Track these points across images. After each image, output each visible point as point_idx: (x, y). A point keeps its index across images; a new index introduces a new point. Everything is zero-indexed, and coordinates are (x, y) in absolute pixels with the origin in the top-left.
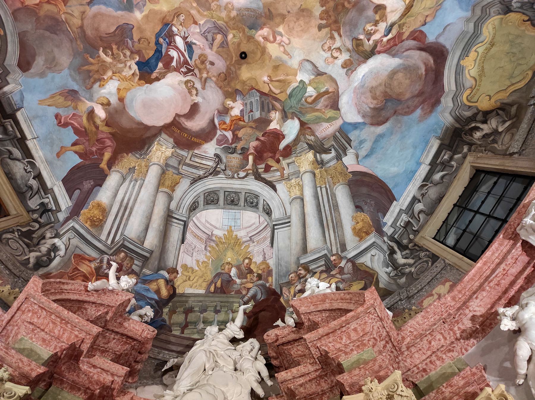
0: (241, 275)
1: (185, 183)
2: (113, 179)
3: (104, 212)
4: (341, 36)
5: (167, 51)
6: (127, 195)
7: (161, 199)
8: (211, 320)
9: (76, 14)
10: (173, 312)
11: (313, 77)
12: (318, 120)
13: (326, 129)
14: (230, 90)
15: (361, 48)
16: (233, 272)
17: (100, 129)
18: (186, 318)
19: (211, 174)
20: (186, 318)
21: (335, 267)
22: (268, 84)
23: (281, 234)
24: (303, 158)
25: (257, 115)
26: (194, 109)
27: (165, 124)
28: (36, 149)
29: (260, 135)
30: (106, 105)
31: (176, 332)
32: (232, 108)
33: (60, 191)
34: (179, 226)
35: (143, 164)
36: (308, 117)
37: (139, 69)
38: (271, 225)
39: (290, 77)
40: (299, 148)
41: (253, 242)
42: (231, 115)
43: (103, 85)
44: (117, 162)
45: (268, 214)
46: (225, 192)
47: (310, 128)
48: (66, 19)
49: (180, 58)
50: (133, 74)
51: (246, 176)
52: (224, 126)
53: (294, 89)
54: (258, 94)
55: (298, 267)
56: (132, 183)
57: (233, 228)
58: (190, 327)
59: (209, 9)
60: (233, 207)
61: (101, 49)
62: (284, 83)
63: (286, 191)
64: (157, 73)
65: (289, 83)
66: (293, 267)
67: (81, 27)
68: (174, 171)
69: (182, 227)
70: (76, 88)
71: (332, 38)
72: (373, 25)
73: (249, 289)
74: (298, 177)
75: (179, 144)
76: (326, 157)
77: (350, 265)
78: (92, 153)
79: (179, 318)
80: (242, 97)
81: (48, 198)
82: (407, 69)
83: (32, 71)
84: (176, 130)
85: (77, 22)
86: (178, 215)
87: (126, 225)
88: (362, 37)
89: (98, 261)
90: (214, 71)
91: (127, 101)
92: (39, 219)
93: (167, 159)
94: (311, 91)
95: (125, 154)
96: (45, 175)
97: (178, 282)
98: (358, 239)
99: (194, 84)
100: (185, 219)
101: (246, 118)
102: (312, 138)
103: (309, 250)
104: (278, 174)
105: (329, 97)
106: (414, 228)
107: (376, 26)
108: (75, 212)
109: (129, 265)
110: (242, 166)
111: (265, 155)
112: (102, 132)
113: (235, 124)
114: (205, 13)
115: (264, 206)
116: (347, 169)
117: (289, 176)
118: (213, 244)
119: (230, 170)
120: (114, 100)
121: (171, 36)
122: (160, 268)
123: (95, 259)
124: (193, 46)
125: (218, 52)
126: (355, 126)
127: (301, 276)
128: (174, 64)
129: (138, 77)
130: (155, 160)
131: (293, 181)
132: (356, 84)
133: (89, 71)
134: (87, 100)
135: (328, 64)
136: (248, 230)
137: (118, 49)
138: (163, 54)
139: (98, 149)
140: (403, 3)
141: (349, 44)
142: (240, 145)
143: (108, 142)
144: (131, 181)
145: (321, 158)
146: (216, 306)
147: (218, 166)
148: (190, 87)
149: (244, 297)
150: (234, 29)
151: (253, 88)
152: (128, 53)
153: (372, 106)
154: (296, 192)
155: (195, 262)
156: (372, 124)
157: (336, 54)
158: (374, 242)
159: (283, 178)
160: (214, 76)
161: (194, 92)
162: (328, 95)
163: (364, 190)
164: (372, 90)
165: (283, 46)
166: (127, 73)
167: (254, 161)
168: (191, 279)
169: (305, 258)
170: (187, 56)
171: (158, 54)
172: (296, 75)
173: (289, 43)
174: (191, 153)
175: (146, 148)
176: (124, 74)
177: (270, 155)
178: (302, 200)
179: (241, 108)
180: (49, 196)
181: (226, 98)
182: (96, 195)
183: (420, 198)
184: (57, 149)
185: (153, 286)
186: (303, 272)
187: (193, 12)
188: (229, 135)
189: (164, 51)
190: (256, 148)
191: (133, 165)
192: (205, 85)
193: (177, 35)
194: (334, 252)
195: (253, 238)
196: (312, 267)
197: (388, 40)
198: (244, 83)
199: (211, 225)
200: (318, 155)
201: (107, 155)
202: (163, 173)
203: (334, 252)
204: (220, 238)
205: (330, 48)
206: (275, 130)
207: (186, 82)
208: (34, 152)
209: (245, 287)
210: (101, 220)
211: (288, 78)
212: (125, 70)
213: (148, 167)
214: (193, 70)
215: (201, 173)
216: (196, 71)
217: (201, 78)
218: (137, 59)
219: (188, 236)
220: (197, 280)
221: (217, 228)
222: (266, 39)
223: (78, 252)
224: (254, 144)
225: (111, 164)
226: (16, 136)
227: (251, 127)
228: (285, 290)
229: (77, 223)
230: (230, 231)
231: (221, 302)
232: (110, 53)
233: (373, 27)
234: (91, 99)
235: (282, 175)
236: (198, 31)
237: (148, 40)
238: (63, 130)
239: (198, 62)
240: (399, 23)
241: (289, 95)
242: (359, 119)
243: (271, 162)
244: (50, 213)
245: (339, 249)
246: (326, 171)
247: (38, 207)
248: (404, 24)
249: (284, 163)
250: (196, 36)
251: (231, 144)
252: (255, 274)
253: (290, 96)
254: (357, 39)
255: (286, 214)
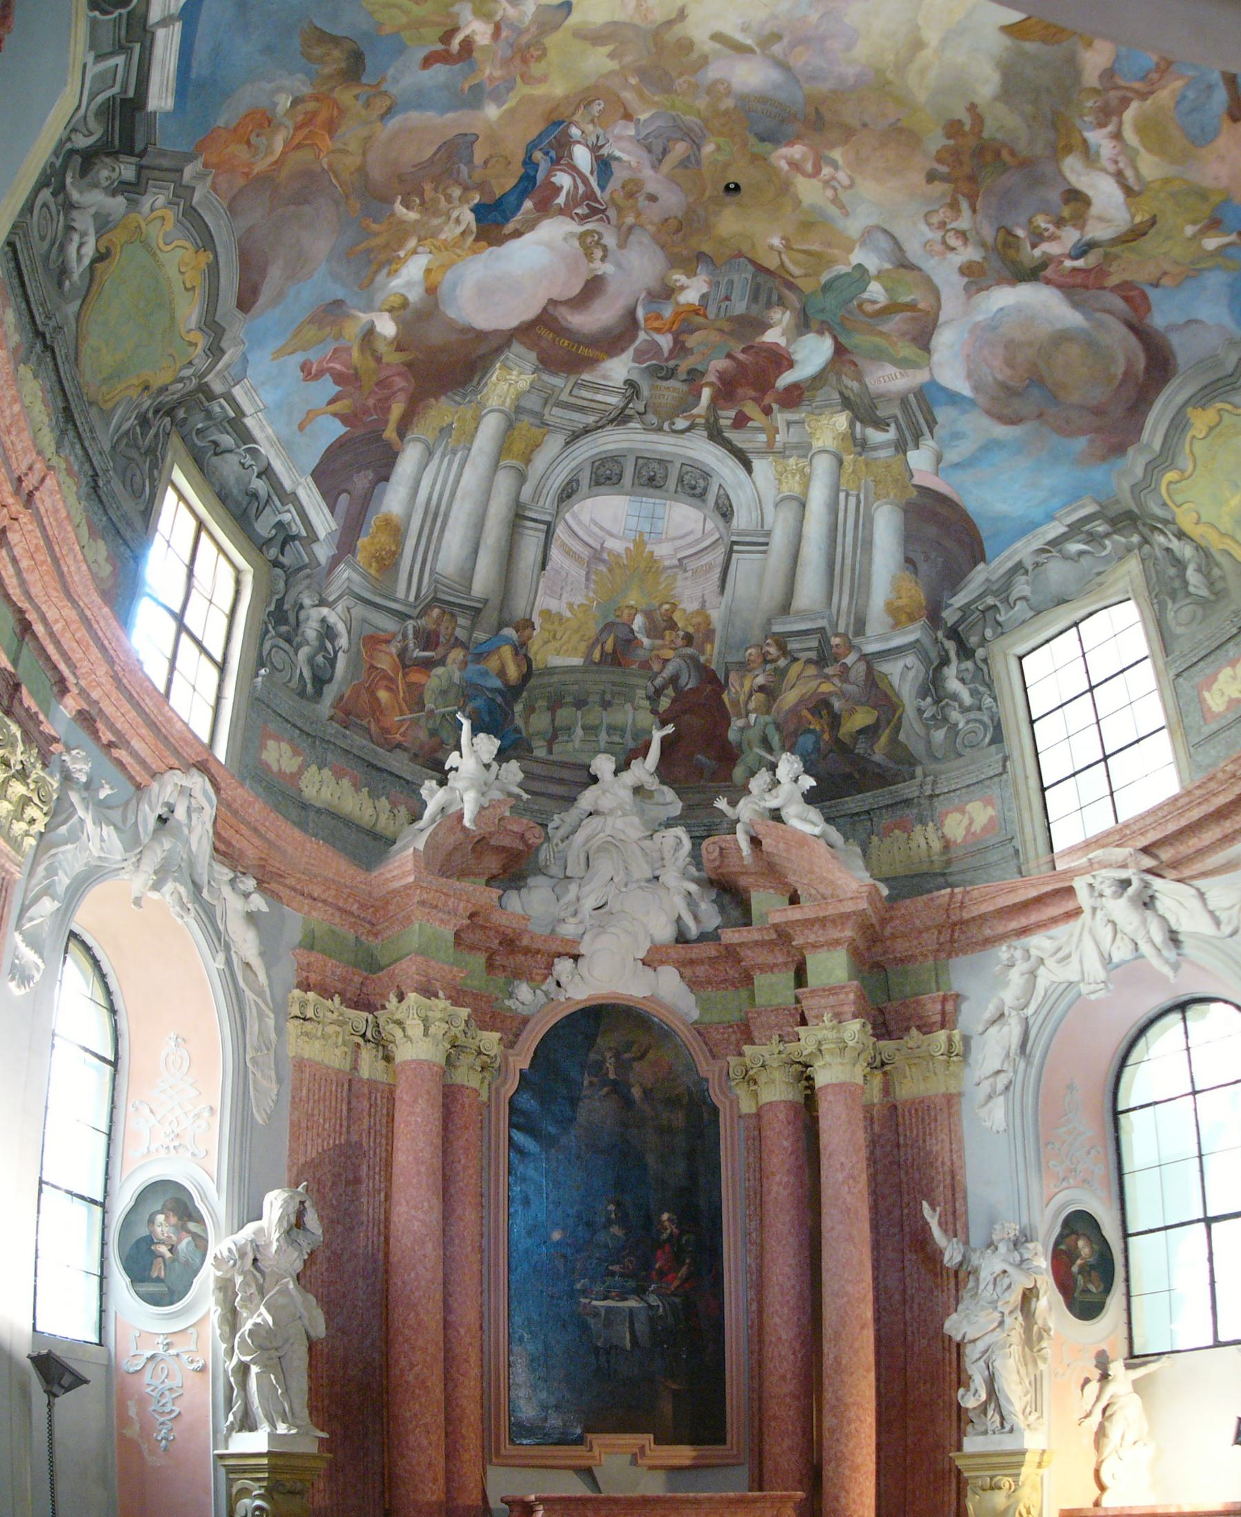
0: (653, 631)
1: (554, 444)
2: (408, 460)
3: (397, 531)
4: (974, 211)
5: (550, 173)
6: (438, 487)
7: (504, 482)
8: (598, 722)
9: (353, 146)
10: (530, 709)
11: (887, 266)
12: (879, 355)
13: (891, 378)
14: (685, 252)
15: (1011, 253)
16: (638, 622)
17: (384, 360)
18: (553, 720)
19: (611, 421)
20: (553, 720)
21: (836, 661)
22: (780, 253)
23: (744, 564)
24: (824, 420)
25: (740, 306)
26: (593, 288)
27: (522, 323)
28: (262, 428)
29: (737, 348)
30: (399, 309)
31: (540, 753)
32: (682, 288)
33: (310, 496)
34: (536, 533)
35: (469, 415)
36: (858, 340)
37: (478, 220)
38: (727, 540)
39: (836, 251)
40: (821, 395)
41: (685, 571)
42: (677, 303)
43: (396, 271)
44: (415, 419)
45: (724, 515)
46: (637, 458)
47: (856, 365)
48: (330, 165)
49: (576, 187)
50: (463, 233)
51: (688, 429)
52: (656, 324)
53: (839, 277)
54: (750, 268)
55: (766, 638)
56: (446, 460)
57: (646, 537)
58: (560, 739)
59: (668, 90)
60: (651, 491)
61: (400, 198)
62: (819, 260)
63: (772, 478)
64: (519, 221)
65: (831, 262)
66: (757, 634)
67: (361, 170)
68: (532, 420)
69: (542, 536)
70: (340, 293)
71: (954, 206)
72: (1049, 222)
73: (666, 661)
74: (805, 456)
75: (548, 363)
76: (875, 436)
77: (862, 667)
78: (366, 411)
79: (540, 721)
80: (711, 267)
81: (289, 511)
82: (1090, 344)
83: (262, 300)
84: (543, 332)
85: (352, 161)
86: (536, 511)
87: (437, 552)
88: (1020, 233)
89: (400, 637)
90: (653, 213)
91: (444, 290)
92: (281, 559)
93: (520, 396)
94: (875, 291)
95: (432, 400)
96: (278, 466)
97: (534, 648)
98: (890, 621)
99: (600, 238)
100: (548, 518)
101: (711, 312)
102: (855, 385)
103: (793, 609)
104: (763, 437)
105: (913, 319)
106: (998, 617)
107: (1058, 228)
108: (346, 544)
109: (449, 631)
110: (684, 406)
111: (740, 391)
112: (388, 365)
113: (684, 320)
114: (656, 98)
115: (718, 497)
116: (912, 476)
117: (785, 448)
118: (602, 568)
119: (656, 413)
120: (415, 295)
121: (560, 150)
122: (502, 625)
123: (394, 635)
124: (614, 165)
125: (671, 179)
126: (954, 398)
127: (769, 657)
128: (561, 200)
129: (473, 237)
130: (494, 402)
131: (792, 461)
132: (980, 318)
133: (369, 251)
134: (360, 310)
135: (931, 253)
136: (679, 543)
137: (436, 190)
138: (538, 183)
139: (379, 400)
140: (1127, 217)
141: (988, 233)
142: (685, 365)
143: (400, 383)
144: (443, 456)
145: (863, 433)
146: (604, 692)
147: (631, 405)
148: (589, 245)
149: (655, 678)
150: (721, 134)
151: (740, 254)
152: (456, 192)
153: (1000, 377)
154: (793, 486)
155: (564, 606)
156: (989, 413)
157: (952, 241)
158: (917, 641)
159: (769, 449)
160: (651, 223)
161: (598, 253)
162: (914, 314)
163: (932, 531)
164: (1011, 346)
165: (835, 189)
166: (450, 232)
167: (714, 400)
168: (558, 636)
169: (784, 623)
170: (594, 183)
171: (527, 184)
172: (851, 250)
173: (851, 186)
174: (573, 379)
175: (476, 379)
176: (443, 236)
177: (752, 393)
178: (803, 505)
179: (705, 289)
180: (290, 507)
181: (673, 267)
182: (381, 502)
183: (1030, 568)
184: (298, 417)
185: (493, 664)
186: (773, 650)
187: (628, 96)
188: (665, 342)
189: (540, 177)
190: (722, 375)
191: (447, 420)
192: (626, 241)
193: (579, 142)
194: (841, 630)
195: (685, 561)
196: (793, 645)
197: (1074, 270)
198: (722, 241)
199: (601, 528)
200: (858, 425)
201: (397, 410)
202: (510, 427)
203: (841, 630)
204: (619, 555)
205: (942, 225)
206: (774, 347)
207: (582, 237)
208: (257, 433)
209: (658, 657)
210: (394, 553)
211: (830, 251)
212: (446, 229)
213: (478, 420)
214: (603, 211)
215: (591, 419)
216: (612, 213)
217: (619, 227)
218: (476, 201)
219: (555, 553)
220: (570, 638)
221: (611, 535)
222: (795, 165)
223: (368, 631)
224: (719, 364)
225: (403, 428)
226: (227, 416)
227: (721, 330)
228: (733, 677)
229: (355, 570)
230: (640, 543)
231: (614, 684)
232: (418, 201)
233: (1051, 227)
234: (369, 308)
235: (771, 443)
236: (632, 133)
237: (506, 158)
238: (312, 384)
239: (620, 197)
240: (1108, 250)
241: (825, 285)
242: (965, 389)
243: (751, 409)
244: (297, 542)
245: (851, 628)
246: (867, 465)
247: (274, 532)
248: (1116, 257)
249: (781, 417)
250: (624, 144)
251: (667, 360)
252: (681, 633)
253: (826, 288)
254: (1009, 233)
255: (762, 526)
